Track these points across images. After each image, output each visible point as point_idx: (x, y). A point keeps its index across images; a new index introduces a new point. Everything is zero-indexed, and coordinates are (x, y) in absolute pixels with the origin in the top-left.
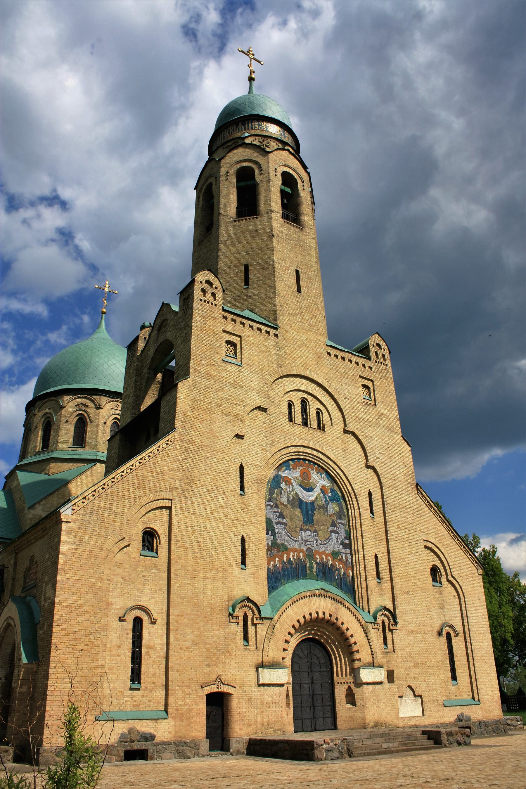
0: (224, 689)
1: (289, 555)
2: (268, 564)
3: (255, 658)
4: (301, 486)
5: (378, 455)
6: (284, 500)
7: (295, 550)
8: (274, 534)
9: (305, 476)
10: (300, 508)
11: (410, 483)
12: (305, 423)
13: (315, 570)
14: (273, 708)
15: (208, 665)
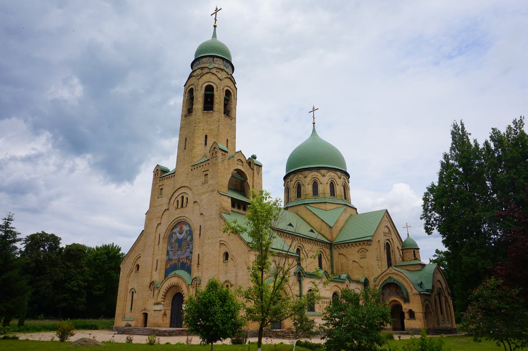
0: (146, 312)
1: (172, 262)
2: (166, 267)
3: (153, 301)
4: (179, 233)
5: (205, 207)
6: (173, 241)
7: (175, 260)
8: (169, 256)
9: (181, 228)
10: (178, 242)
11: (218, 214)
12: (182, 207)
13: (179, 266)
14: (157, 318)
15: (143, 304)
